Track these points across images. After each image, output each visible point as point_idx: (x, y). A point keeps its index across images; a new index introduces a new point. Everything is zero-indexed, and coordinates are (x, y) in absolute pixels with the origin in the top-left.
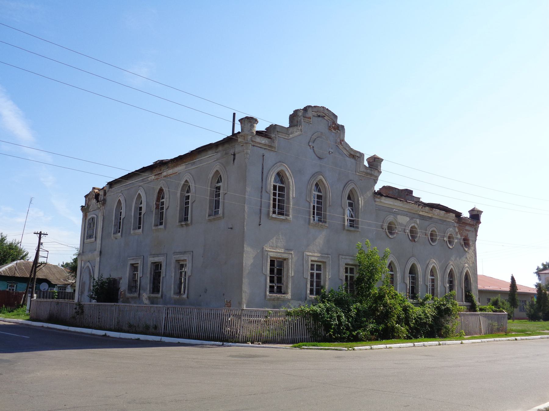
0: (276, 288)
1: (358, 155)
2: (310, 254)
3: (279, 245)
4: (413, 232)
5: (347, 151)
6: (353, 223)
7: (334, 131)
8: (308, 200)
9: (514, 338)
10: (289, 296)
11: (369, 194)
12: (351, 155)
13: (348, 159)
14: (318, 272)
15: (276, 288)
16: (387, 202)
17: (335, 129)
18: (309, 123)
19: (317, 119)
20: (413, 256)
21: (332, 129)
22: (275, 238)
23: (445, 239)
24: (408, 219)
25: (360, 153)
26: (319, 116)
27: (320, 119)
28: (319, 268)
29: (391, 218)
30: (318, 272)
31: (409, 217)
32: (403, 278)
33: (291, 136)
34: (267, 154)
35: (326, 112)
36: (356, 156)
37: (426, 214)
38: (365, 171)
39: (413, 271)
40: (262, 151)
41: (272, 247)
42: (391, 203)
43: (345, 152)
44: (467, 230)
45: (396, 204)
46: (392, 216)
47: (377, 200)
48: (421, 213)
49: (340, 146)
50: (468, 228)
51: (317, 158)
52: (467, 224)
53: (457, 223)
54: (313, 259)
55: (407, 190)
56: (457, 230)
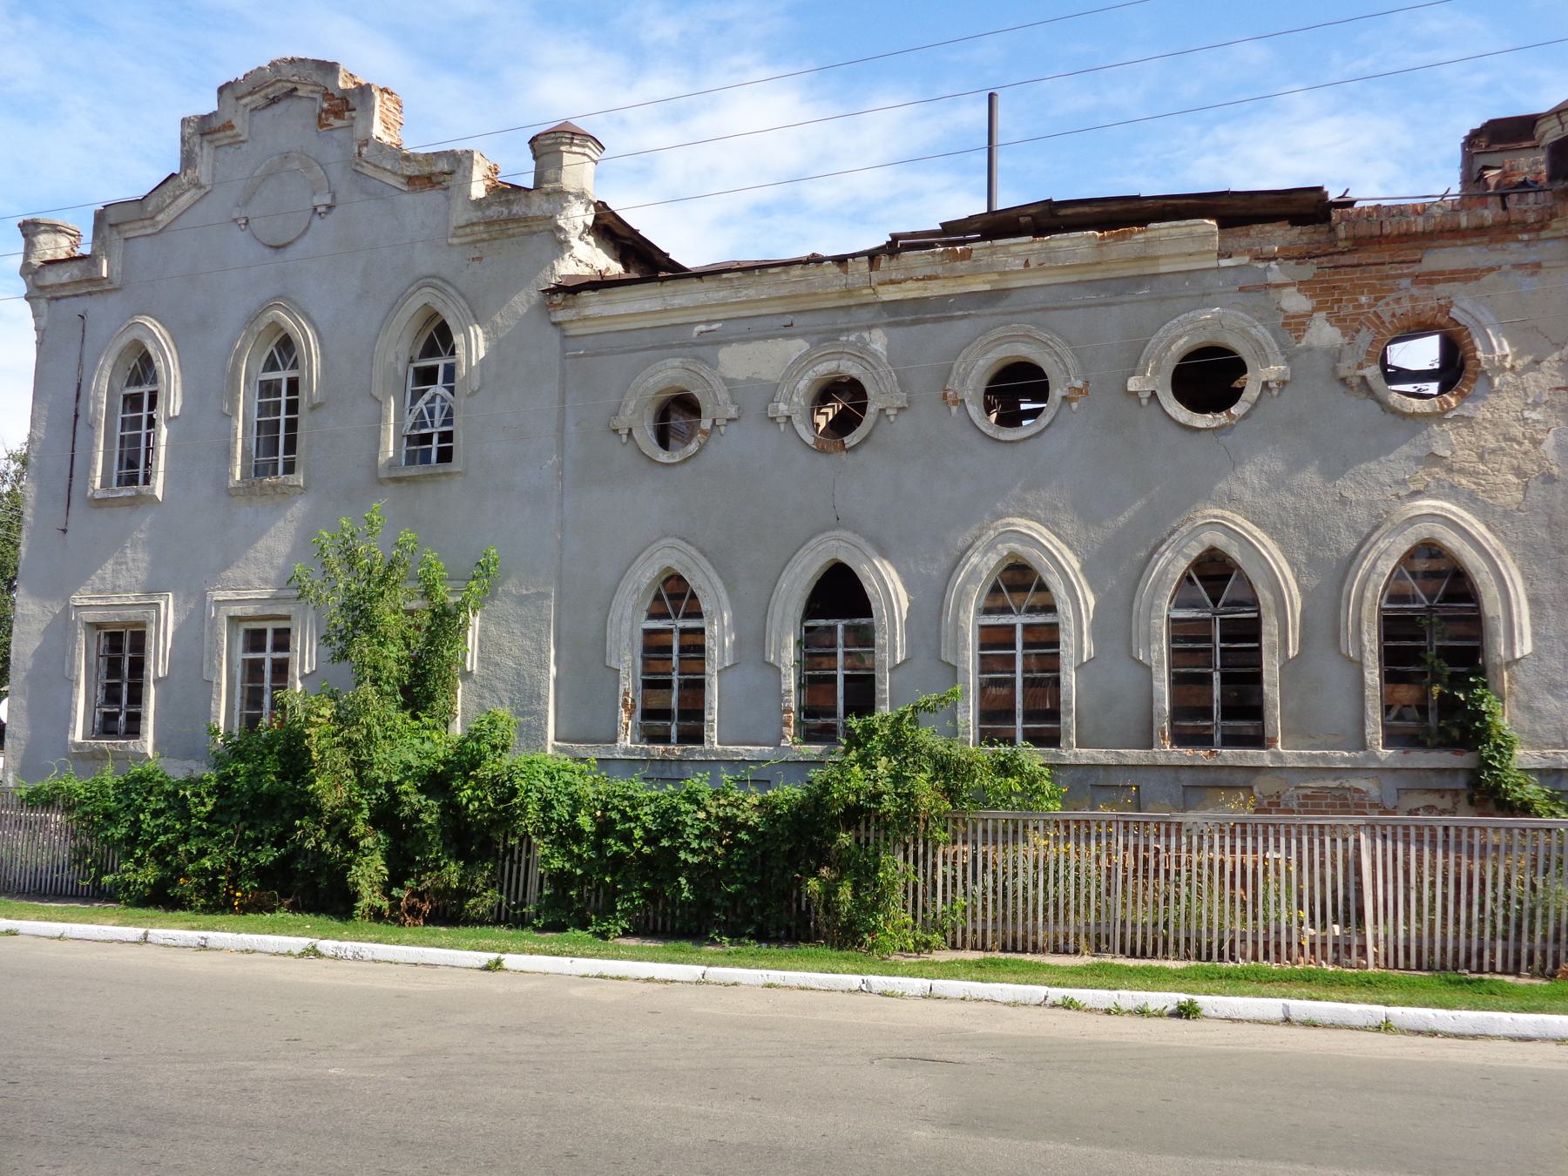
0: (122, 718)
1: (443, 166)
2: (230, 595)
3: (121, 583)
4: (845, 401)
5: (395, 173)
6: (431, 447)
7: (338, 123)
8: (226, 408)
9: (1170, 999)
10: (148, 742)
11: (523, 301)
12: (410, 180)
13: (407, 198)
14: (279, 655)
15: (122, 718)
16: (622, 309)
17: (338, 114)
18: (237, 142)
19: (268, 113)
20: (838, 522)
21: (332, 120)
22: (109, 565)
23: (1133, 384)
24: (798, 346)
25: (451, 155)
26: (274, 101)
27: (279, 109)
28: (283, 640)
29: (668, 374)
30: (279, 655)
31: (803, 335)
32: (753, 643)
33: (160, 217)
34: (95, 307)
35: (287, 71)
36: (437, 174)
37: (934, 289)
38: (475, 215)
39: (839, 594)
40: (79, 305)
41: (99, 591)
42: (648, 305)
43: (391, 180)
44: (1430, 279)
45: (678, 301)
46: (677, 362)
47: (560, 316)
48: (889, 294)
49: (369, 170)
50: (1441, 259)
51: (267, 251)
52: (1407, 237)
53: (1303, 257)
54: (237, 610)
55: (1492, 123)
56: (1295, 302)
